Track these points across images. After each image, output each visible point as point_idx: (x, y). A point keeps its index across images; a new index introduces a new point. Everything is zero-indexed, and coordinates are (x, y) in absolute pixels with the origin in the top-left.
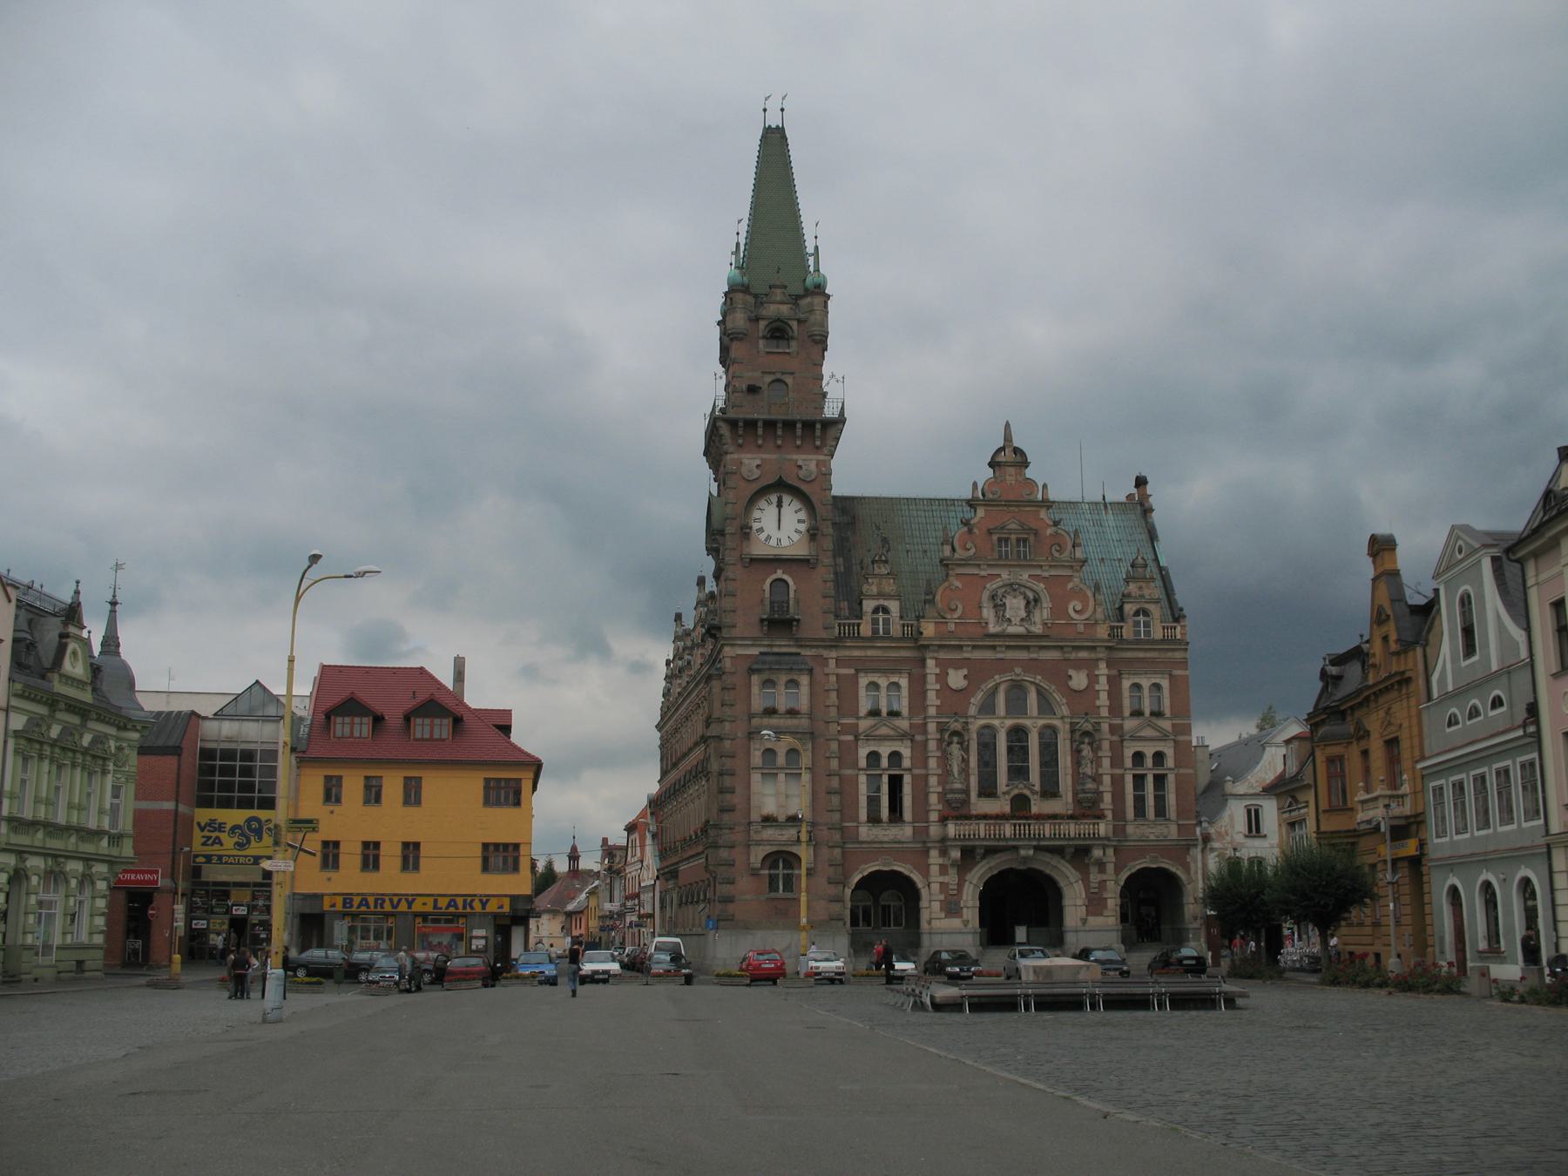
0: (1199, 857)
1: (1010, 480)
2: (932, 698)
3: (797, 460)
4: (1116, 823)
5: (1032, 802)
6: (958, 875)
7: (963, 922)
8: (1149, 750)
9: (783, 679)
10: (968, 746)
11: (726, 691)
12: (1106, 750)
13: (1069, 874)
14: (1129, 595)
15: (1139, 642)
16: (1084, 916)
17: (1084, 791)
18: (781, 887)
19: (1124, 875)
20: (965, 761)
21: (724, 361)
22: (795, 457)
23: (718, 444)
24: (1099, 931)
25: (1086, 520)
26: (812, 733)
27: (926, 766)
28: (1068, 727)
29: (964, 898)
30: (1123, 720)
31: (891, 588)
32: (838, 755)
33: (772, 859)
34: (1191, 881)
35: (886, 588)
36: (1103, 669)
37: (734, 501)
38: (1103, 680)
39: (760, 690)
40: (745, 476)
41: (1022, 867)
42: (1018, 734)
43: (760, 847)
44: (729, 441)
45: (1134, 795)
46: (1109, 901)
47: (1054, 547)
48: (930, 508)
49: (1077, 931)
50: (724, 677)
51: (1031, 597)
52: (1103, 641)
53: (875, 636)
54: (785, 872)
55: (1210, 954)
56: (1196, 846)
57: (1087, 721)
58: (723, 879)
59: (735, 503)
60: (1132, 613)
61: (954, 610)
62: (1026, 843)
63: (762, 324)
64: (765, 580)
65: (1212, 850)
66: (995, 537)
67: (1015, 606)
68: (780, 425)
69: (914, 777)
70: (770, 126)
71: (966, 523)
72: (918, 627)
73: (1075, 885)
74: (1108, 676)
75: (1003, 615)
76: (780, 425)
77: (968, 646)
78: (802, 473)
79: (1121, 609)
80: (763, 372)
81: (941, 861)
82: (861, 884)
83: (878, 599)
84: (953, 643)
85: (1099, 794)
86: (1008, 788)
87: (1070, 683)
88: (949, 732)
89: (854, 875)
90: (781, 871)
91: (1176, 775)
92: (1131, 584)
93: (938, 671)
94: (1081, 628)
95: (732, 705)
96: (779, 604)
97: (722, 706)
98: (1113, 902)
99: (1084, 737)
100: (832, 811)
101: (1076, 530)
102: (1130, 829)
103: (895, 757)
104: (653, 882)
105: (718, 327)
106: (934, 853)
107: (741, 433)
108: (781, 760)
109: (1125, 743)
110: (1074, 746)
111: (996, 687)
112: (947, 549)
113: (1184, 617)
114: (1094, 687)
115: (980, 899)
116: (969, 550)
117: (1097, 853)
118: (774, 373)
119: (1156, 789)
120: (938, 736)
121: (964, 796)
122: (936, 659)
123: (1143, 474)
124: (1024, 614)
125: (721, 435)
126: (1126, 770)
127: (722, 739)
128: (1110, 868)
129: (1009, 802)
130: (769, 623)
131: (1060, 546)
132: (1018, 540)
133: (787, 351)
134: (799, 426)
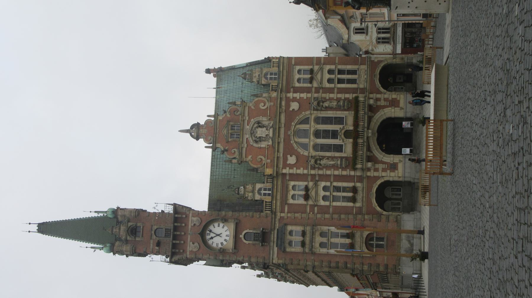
0: (375, 56)
2: (300, 171)
4: (359, 92)
5: (348, 129)
6: (379, 164)
7: (400, 162)
8: (327, 76)
9: (289, 237)
10: (321, 156)
11: (293, 263)
12: (327, 96)
13: (380, 115)
14: (258, 82)
15: (279, 78)
16: (399, 108)
17: (344, 106)
18: (381, 243)
19: (382, 90)
20: (328, 158)
21: (144, 255)
22: (190, 227)
23: (182, 261)
25: (224, 97)
26: (313, 226)
27: (330, 175)
28: (315, 112)
29: (389, 161)
30: (313, 87)
31: (250, 187)
32: (323, 215)
33: (369, 246)
34: (386, 60)
36: (290, 95)
37: (208, 255)
38: (295, 95)
39: (293, 248)
40: (197, 250)
41: (376, 135)
42: (317, 134)
44: (181, 256)
45: (346, 84)
46: (393, 97)
47: (236, 114)
49: (406, 112)
50: (287, 263)
51: (257, 125)
52: (277, 95)
53: (271, 195)
54: (375, 240)
55: (419, 53)
56: (370, 57)
57: (313, 103)
58: (377, 269)
59: (209, 254)
60: (266, 81)
61: (261, 159)
62: (365, 133)
63: (128, 238)
64: (244, 243)
65: (373, 50)
67: (261, 132)
68: (176, 233)
69: (335, 181)
70: (37, 230)
71: (223, 152)
72: (268, 175)
73: (385, 112)
74: (293, 93)
75: (264, 138)
76: (176, 233)
77: (277, 154)
78: (198, 224)
79: (264, 85)
80: (151, 239)
81: (372, 171)
82: (381, 206)
83: (255, 193)
85: (345, 99)
86: (341, 139)
87: (296, 110)
89: (377, 210)
90: (374, 242)
91: (338, 65)
92: (253, 81)
93: (288, 168)
94: (272, 104)
95: (299, 261)
96: (256, 237)
97: (299, 265)
99: (320, 105)
100: (348, 218)
101: (228, 103)
102: (361, 86)
103: (325, 189)
104: (378, 292)
105: (129, 257)
106: (369, 174)
107: (177, 251)
108: (324, 240)
109: (324, 86)
110: (323, 109)
111: (296, 142)
112: (234, 161)
113: (269, 57)
115: (390, 154)
116: (235, 151)
117: (371, 102)
118: (151, 234)
119: (344, 74)
120: (317, 169)
121: (344, 160)
122: (282, 169)
123: (205, 70)
124: (264, 129)
125: (179, 259)
126: (335, 87)
127: (314, 266)
128: (379, 96)
129: (347, 139)
130: (263, 242)
131: (235, 112)
132: (232, 129)
133: (142, 227)
134: (176, 224)
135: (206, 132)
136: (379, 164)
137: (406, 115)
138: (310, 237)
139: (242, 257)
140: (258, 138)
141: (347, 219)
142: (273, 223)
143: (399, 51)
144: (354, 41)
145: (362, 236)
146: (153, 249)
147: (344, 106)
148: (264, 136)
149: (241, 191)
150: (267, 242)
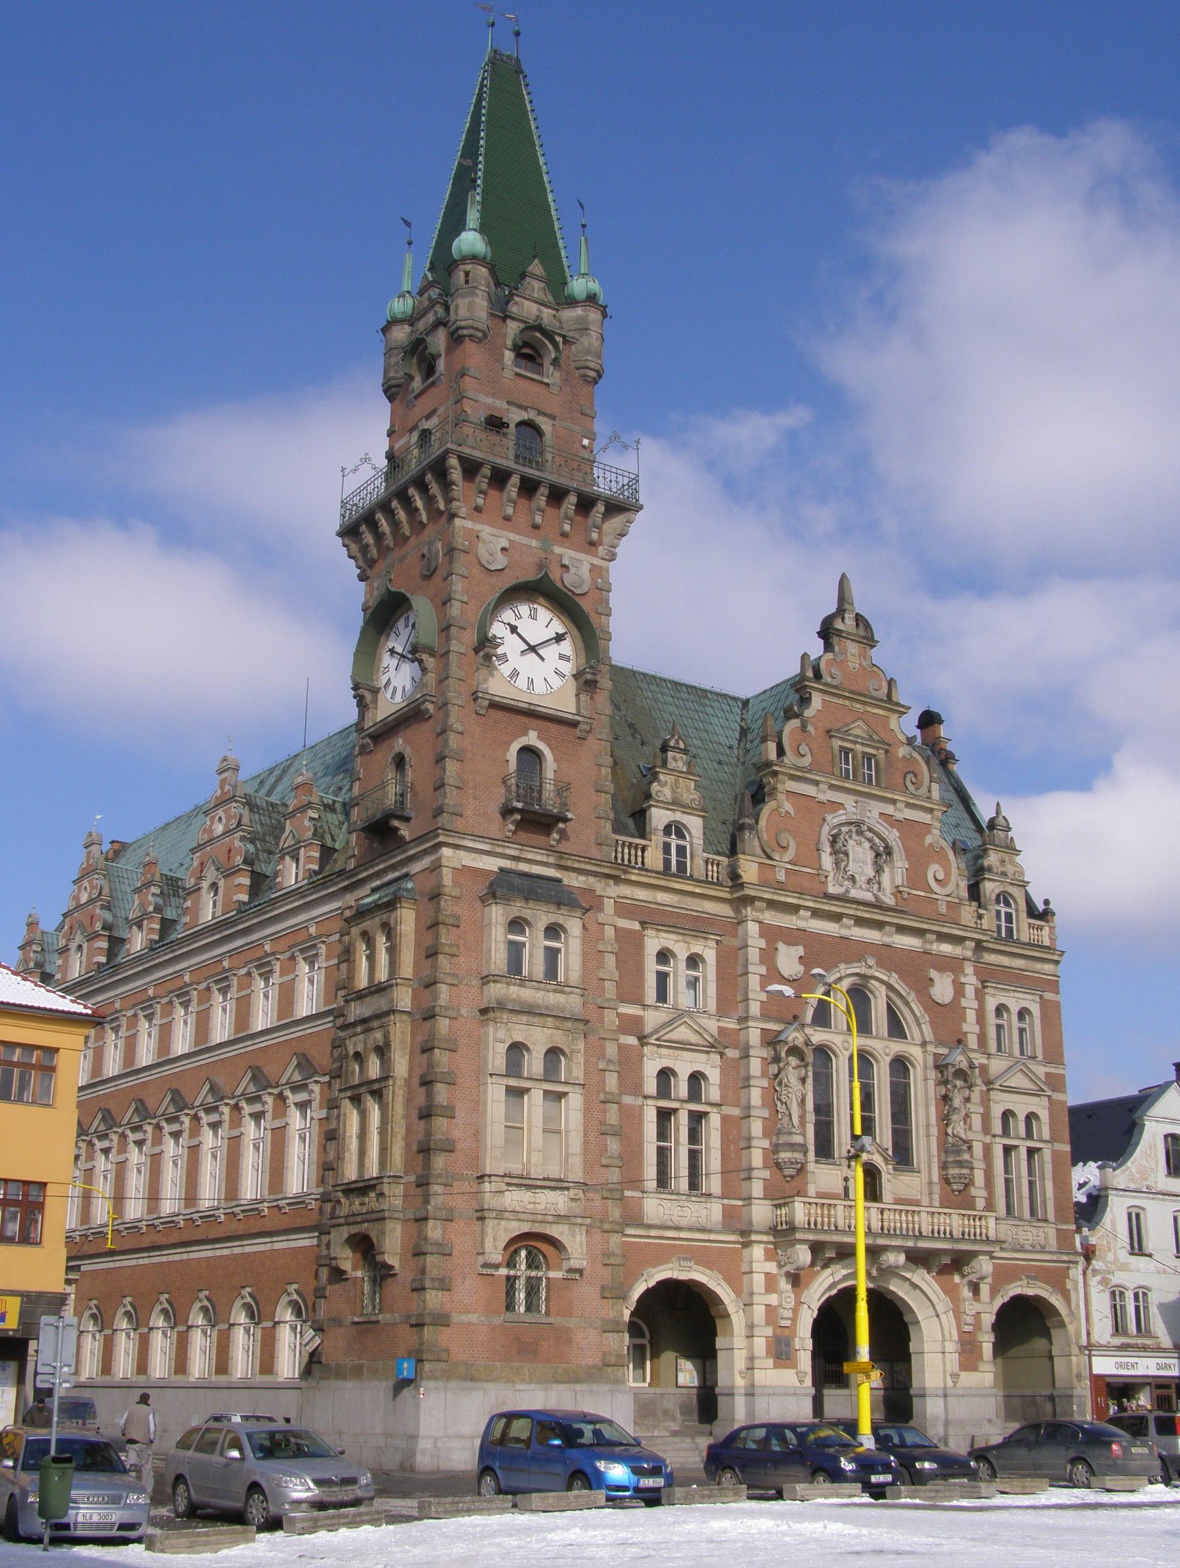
1: (853, 662)
3: (561, 556)
19: (999, 1302)
24: (974, 1396)
28: (930, 1059)
31: (691, 797)
32: (618, 1069)
35: (685, 796)
36: (970, 979)
37: (465, 600)
38: (970, 991)
43: (503, 1223)
46: (984, 1344)
48: (678, 695)
51: (881, 849)
54: (533, 1273)
58: (433, 1280)
59: (466, 603)
60: (994, 897)
61: (785, 848)
64: (508, 744)
66: (837, 743)
67: (860, 855)
68: (543, 491)
69: (725, 1119)
73: (943, 1317)
76: (543, 491)
77: (807, 908)
78: (569, 579)
80: (508, 403)
84: (789, 900)
88: (786, 1048)
89: (636, 1286)
94: (943, 909)
95: (452, 955)
98: (987, 1349)
100: (607, 1166)
108: (535, 1063)
114: (959, 1002)
118: (525, 409)
122: (760, 922)
124: (870, 872)
126: (994, 1136)
131: (915, 775)
133: (546, 380)
135: (849, 663)
136: (792, 1296)
137: (931, 1396)
138: (547, 1008)
139: (460, 729)
140: (844, 846)
141: (604, 1161)
142: (583, 866)
143: (1104, 1366)
144: (1112, 1211)
145: (560, 1218)
146: (476, 401)
147: (960, 1164)
148: (852, 868)
149: (674, 759)
150: (514, 833)
